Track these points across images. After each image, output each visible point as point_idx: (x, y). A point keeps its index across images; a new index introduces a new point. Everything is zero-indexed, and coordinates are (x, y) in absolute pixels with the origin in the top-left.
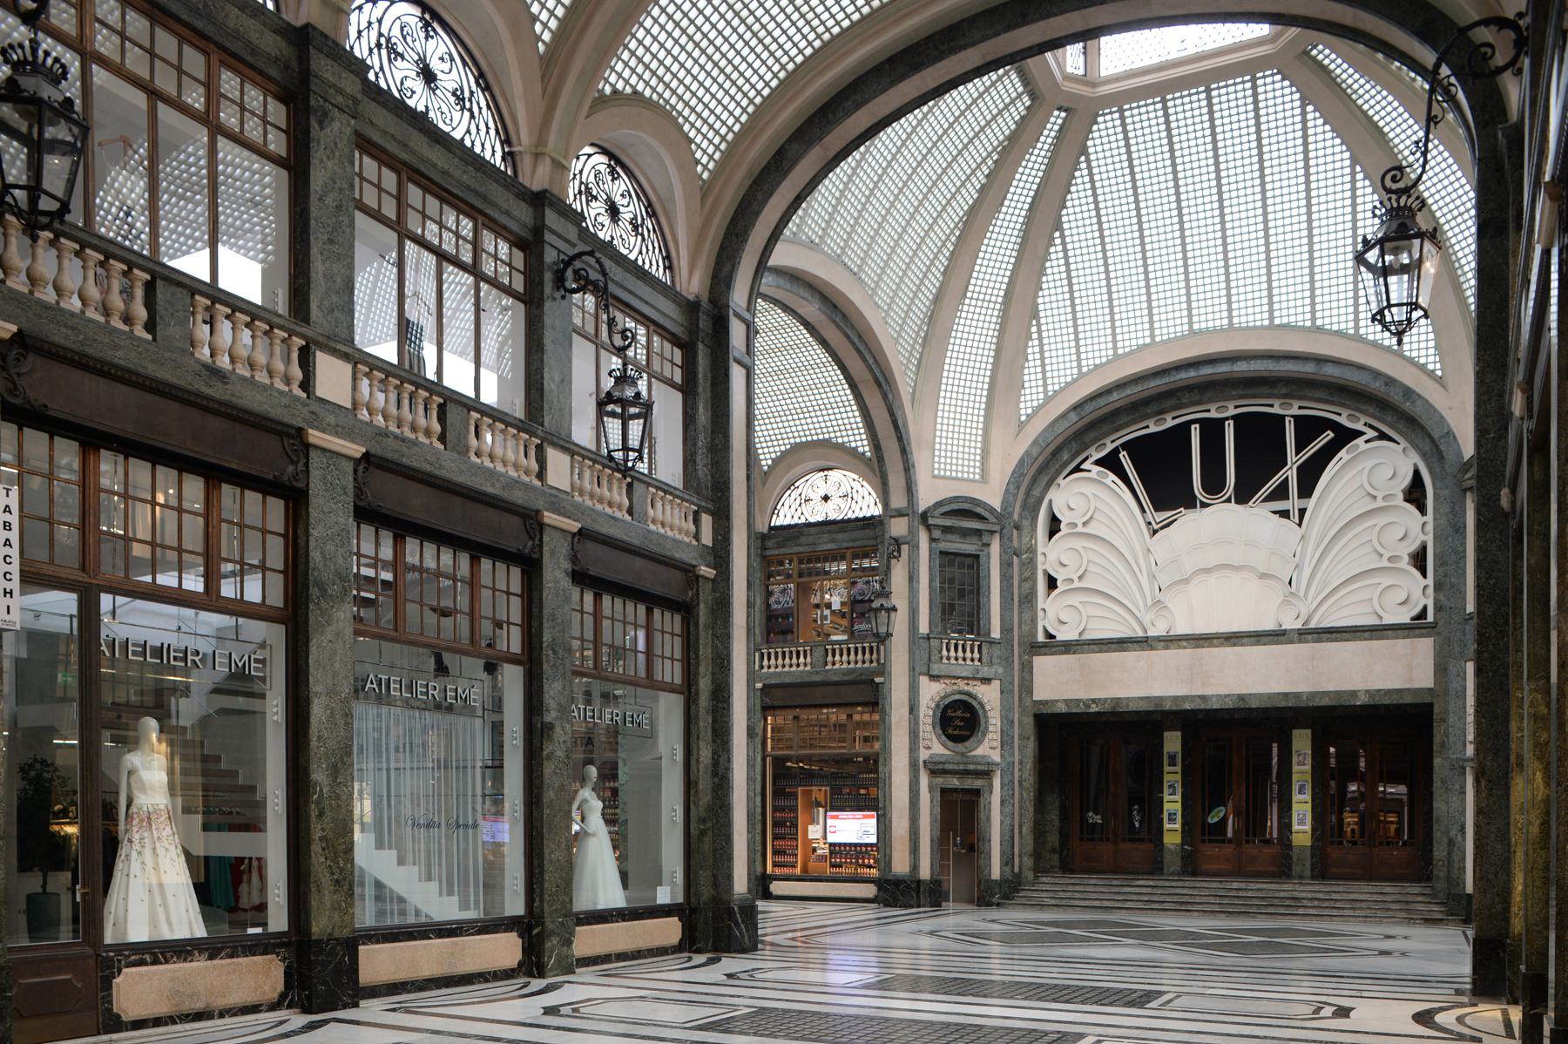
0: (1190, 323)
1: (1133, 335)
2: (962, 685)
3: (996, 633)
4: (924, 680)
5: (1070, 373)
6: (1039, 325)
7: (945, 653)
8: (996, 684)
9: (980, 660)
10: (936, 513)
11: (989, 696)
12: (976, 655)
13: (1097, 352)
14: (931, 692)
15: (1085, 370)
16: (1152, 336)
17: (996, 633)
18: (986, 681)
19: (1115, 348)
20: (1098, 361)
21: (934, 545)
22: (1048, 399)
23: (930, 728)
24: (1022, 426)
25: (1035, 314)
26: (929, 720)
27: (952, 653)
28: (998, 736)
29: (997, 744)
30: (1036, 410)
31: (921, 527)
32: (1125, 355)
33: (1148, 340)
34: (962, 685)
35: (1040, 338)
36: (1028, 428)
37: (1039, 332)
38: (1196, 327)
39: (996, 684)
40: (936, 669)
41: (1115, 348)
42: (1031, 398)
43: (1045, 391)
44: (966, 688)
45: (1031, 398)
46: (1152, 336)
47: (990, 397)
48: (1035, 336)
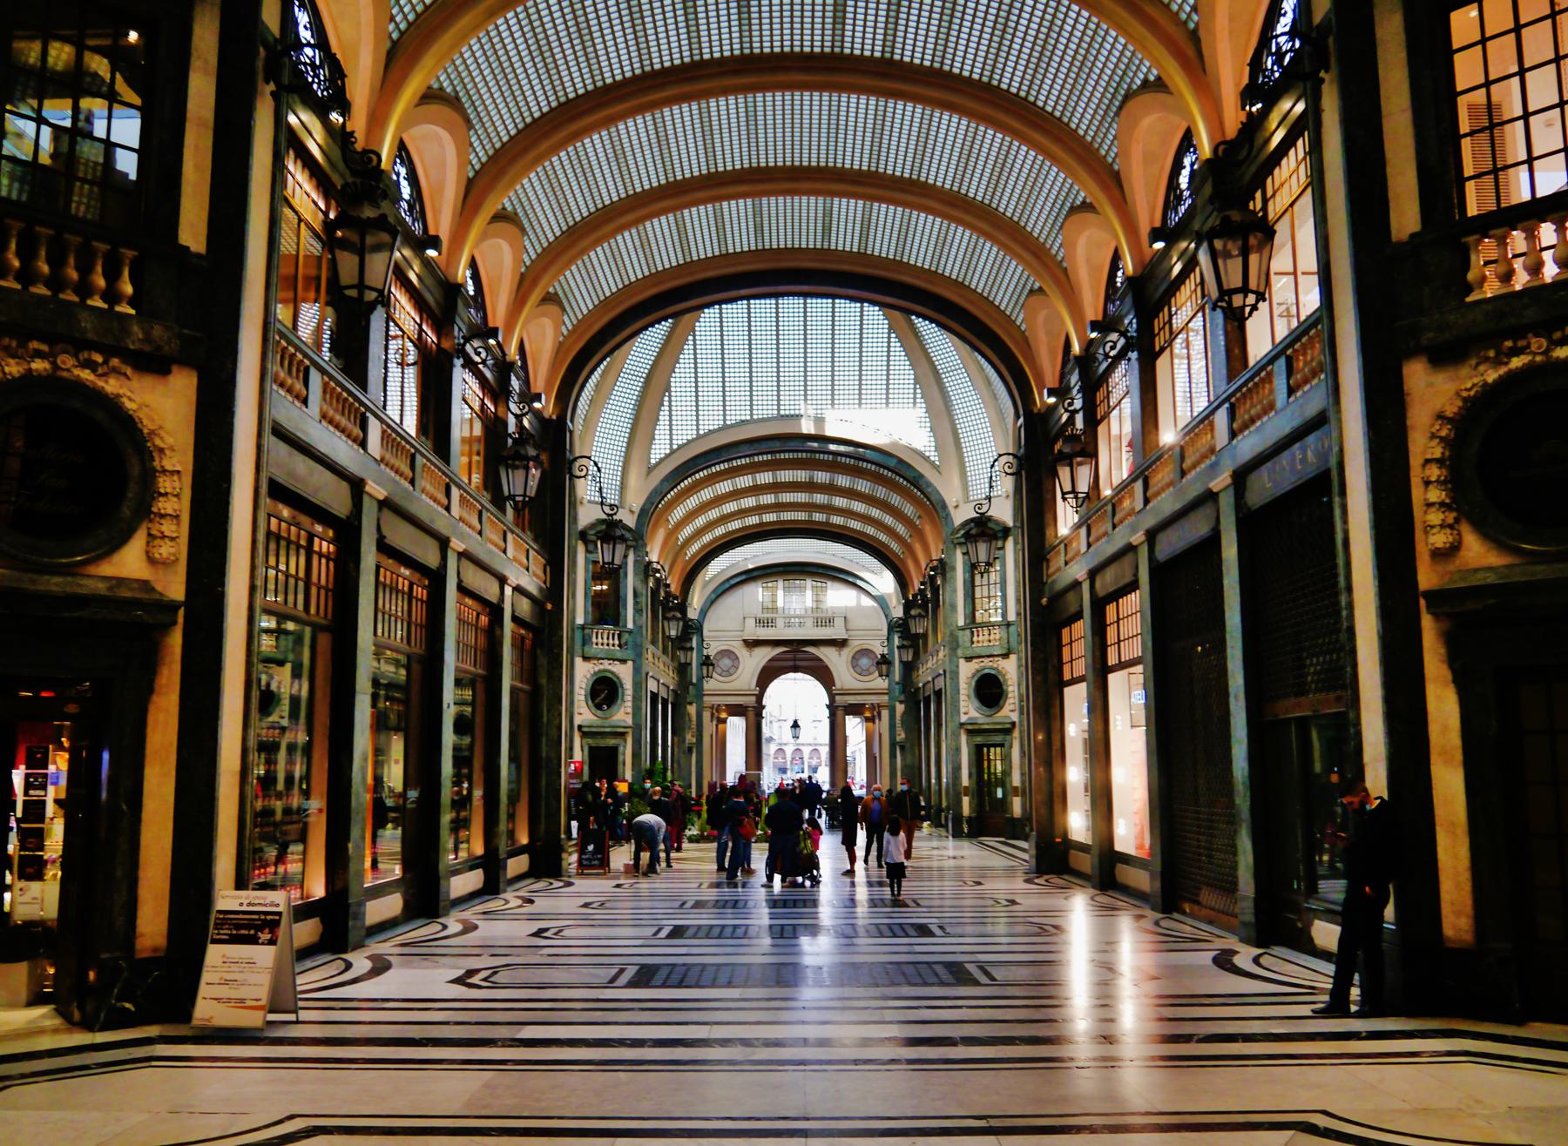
0: (779, 410)
1: (738, 413)
2: (606, 665)
3: (630, 625)
4: (578, 661)
5: (691, 435)
6: (670, 396)
7: (594, 640)
8: (630, 663)
9: (620, 646)
10: (592, 532)
11: (624, 673)
12: (617, 642)
13: (711, 421)
14: (583, 673)
15: (701, 432)
16: (751, 415)
17: (630, 625)
18: (623, 661)
19: (725, 420)
20: (711, 428)
21: (589, 555)
22: (673, 452)
23: (583, 698)
24: (651, 469)
25: (668, 389)
26: (583, 692)
27: (600, 640)
28: (630, 704)
29: (630, 710)
30: (662, 460)
31: (580, 542)
32: (732, 426)
33: (748, 418)
34: (606, 665)
35: (670, 406)
36: (656, 472)
37: (670, 401)
38: (782, 412)
39: (630, 663)
40: (591, 651)
41: (725, 420)
42: (659, 450)
43: (671, 444)
44: (610, 667)
45: (659, 450)
46: (751, 415)
47: (629, 443)
48: (666, 403)
